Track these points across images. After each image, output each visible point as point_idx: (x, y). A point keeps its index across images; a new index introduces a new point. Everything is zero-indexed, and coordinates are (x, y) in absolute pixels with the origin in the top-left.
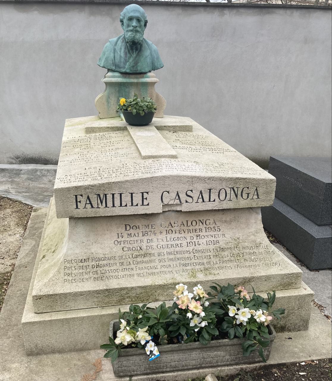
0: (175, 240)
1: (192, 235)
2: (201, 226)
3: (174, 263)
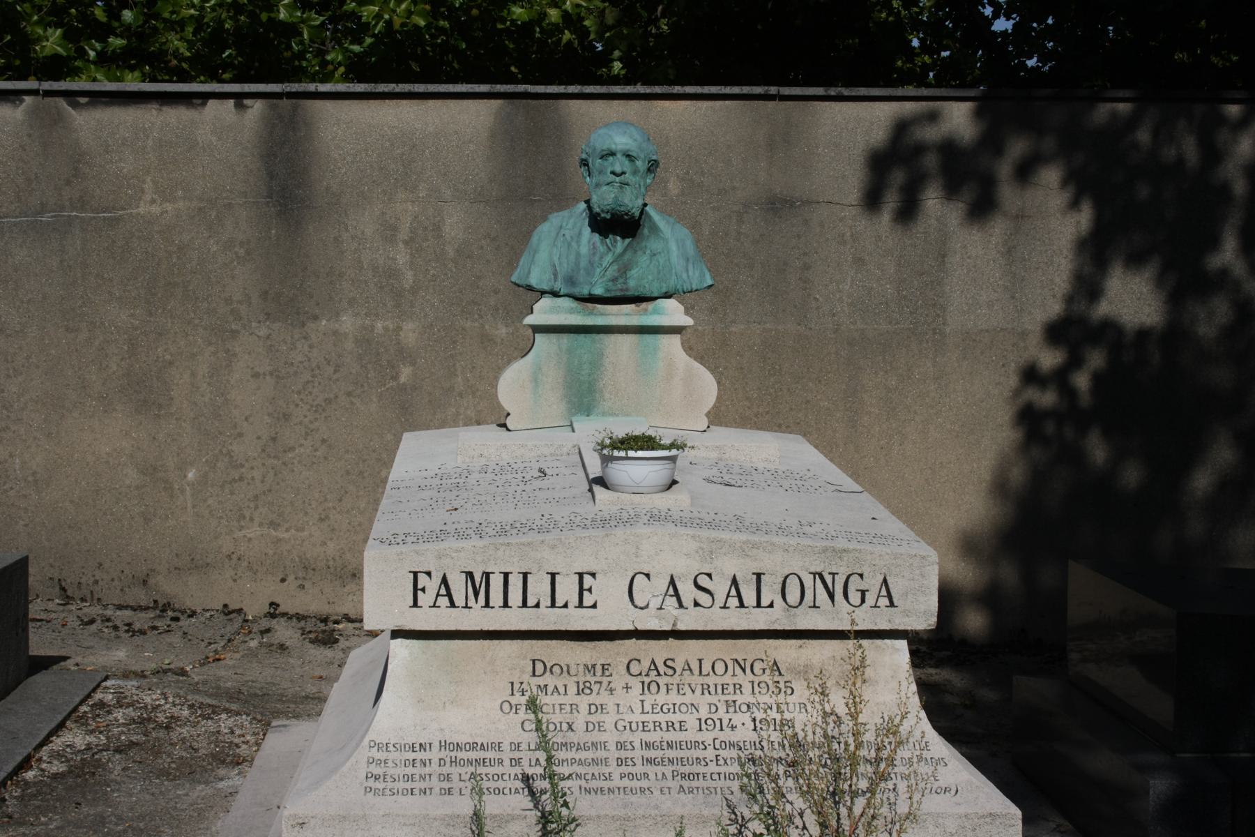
0: (665, 710)
1: (714, 699)
2: (741, 678)
3: (659, 769)
